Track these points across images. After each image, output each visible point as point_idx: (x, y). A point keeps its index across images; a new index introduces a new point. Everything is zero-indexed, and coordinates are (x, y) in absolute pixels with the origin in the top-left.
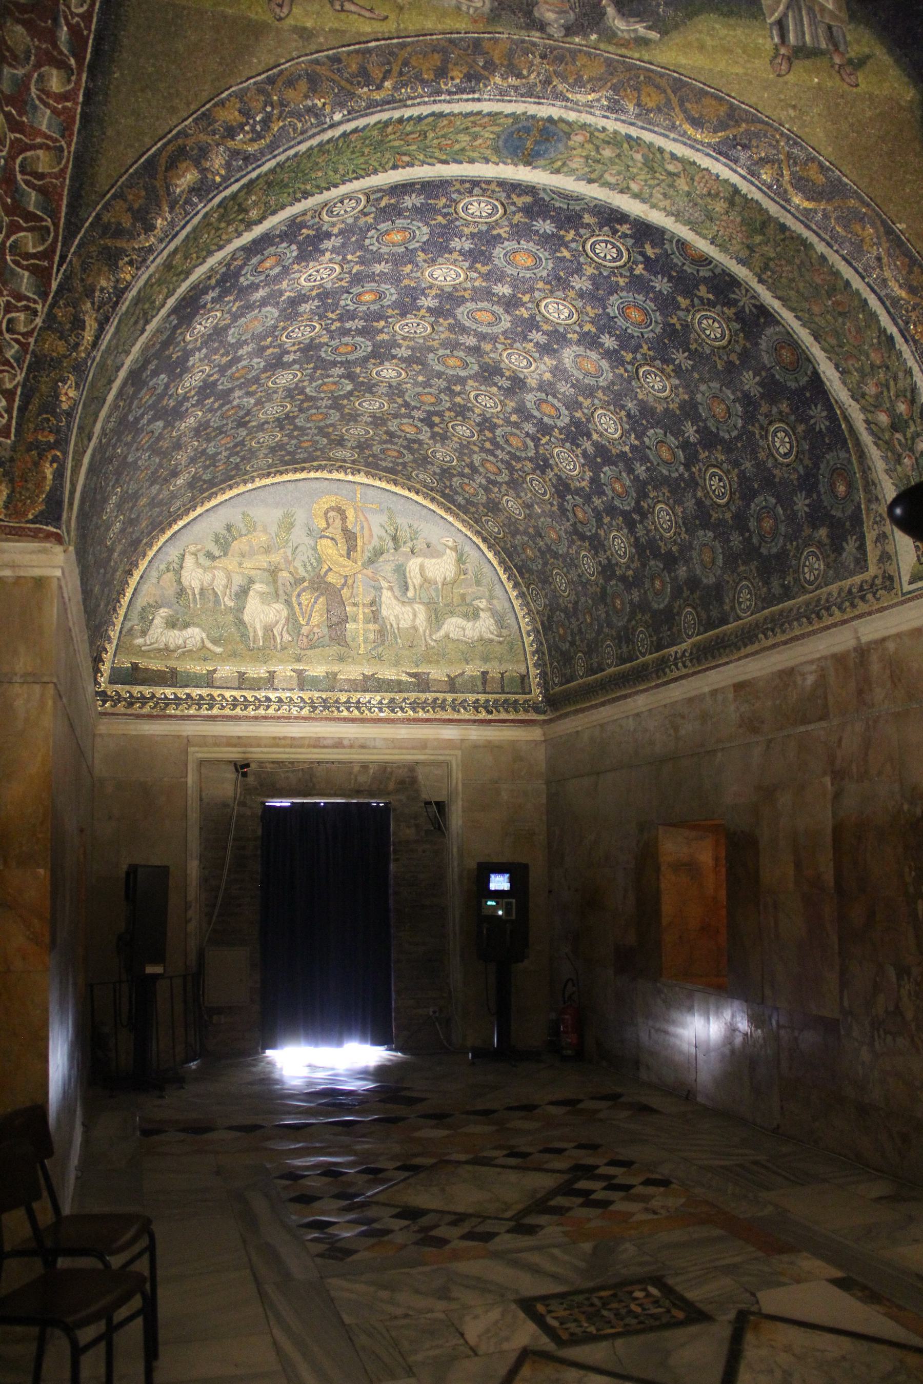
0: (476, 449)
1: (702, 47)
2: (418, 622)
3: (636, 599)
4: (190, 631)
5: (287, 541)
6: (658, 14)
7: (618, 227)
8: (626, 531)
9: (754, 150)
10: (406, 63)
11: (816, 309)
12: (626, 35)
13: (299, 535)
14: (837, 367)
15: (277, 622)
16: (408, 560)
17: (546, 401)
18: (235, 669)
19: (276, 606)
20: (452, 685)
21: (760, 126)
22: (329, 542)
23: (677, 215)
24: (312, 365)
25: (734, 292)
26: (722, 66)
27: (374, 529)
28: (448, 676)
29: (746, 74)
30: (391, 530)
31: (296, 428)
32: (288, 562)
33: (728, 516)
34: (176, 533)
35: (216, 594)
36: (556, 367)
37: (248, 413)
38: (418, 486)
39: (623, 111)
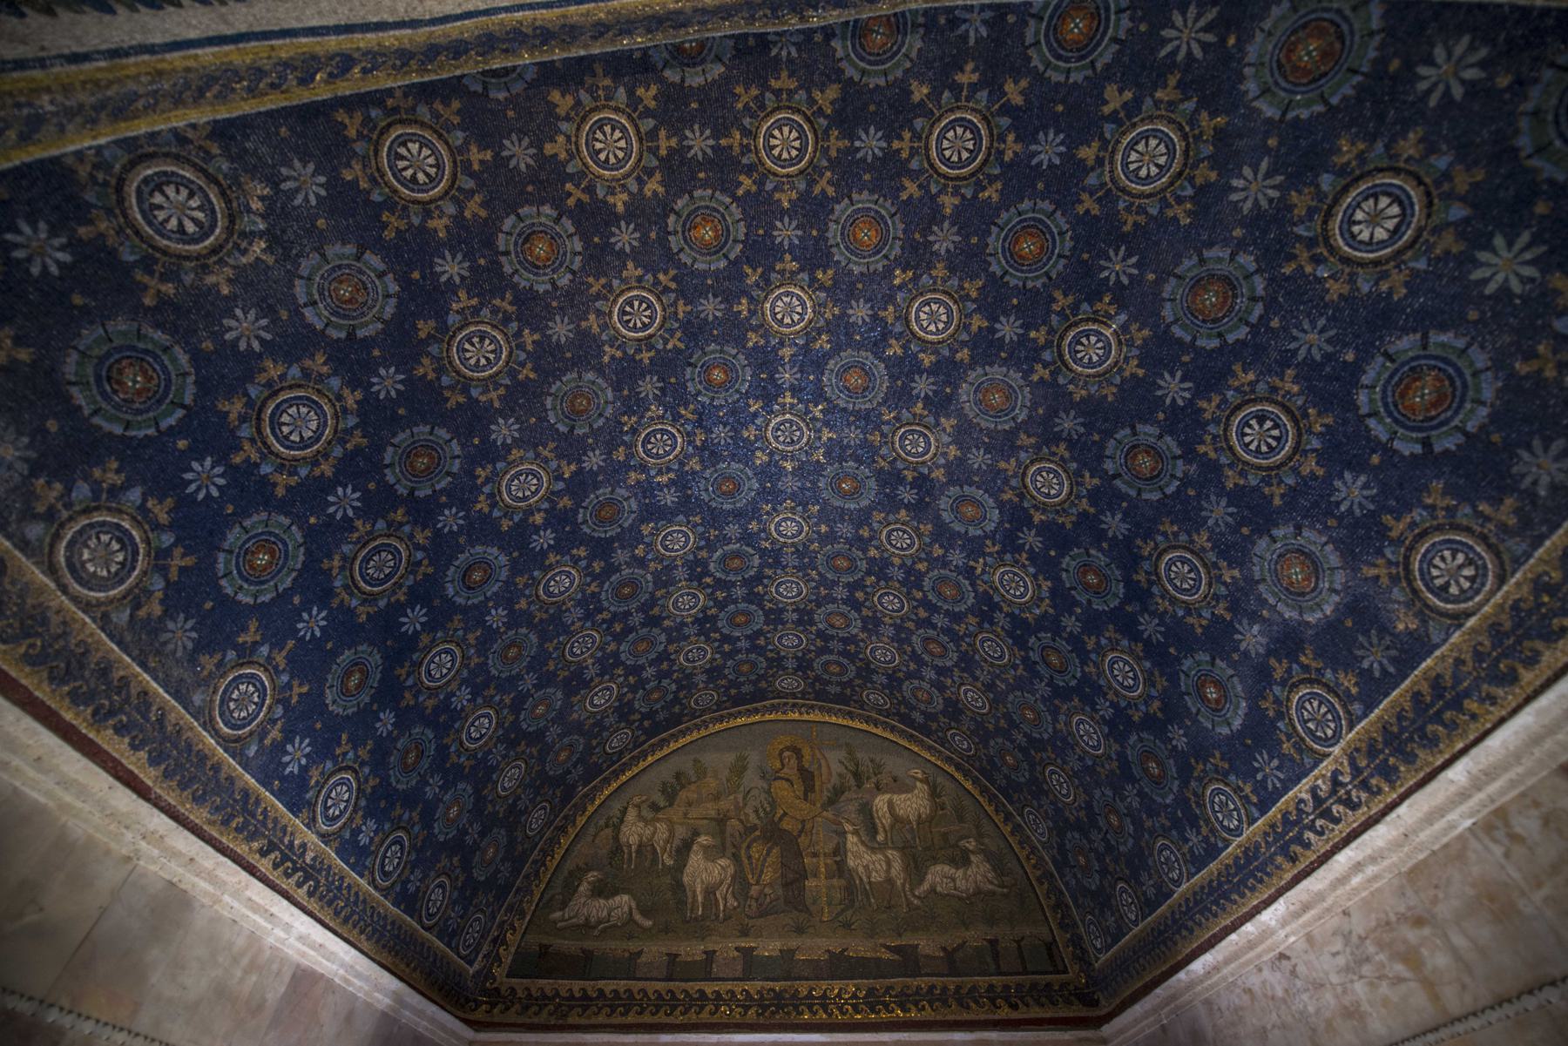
0: (910, 625)
2: (894, 872)
3: (1181, 742)
4: (617, 898)
8: (1125, 643)
13: (751, 779)
16: (874, 797)
17: (963, 499)
18: (664, 950)
19: (723, 862)
20: (952, 962)
22: (786, 785)
24: (698, 519)
27: (833, 764)
28: (944, 949)
31: (726, 639)
32: (737, 808)
33: (1310, 466)
36: (957, 428)
37: (653, 601)
38: (874, 715)
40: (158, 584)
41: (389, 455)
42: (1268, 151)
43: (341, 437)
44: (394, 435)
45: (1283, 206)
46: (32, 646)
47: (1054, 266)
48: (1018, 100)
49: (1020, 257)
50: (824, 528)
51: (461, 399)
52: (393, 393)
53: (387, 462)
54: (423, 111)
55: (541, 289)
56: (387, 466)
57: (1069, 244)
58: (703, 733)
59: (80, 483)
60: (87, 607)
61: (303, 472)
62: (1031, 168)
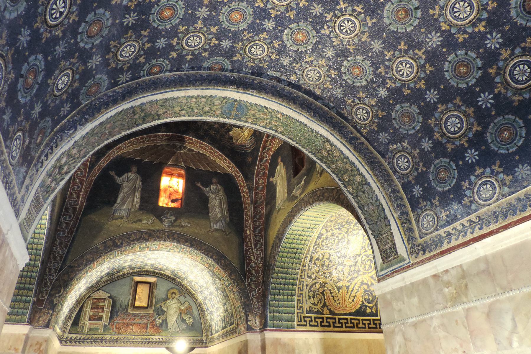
7: (192, 57)
11: (108, 126)
14: (87, 133)
25: (130, 74)
40: (501, 176)
41: (463, 86)
42: (94, 70)
43: (457, 108)
44: (453, 86)
45: (85, 63)
46: (501, 217)
47: (156, 9)
48: (172, 53)
49: (169, 9)
51: (428, 65)
52: (436, 92)
53: (466, 86)
54: (350, 117)
55: (368, 63)
56: (468, 85)
57: (151, 18)
59: (465, 193)
60: (497, 200)
61: (472, 120)
62: (167, 37)
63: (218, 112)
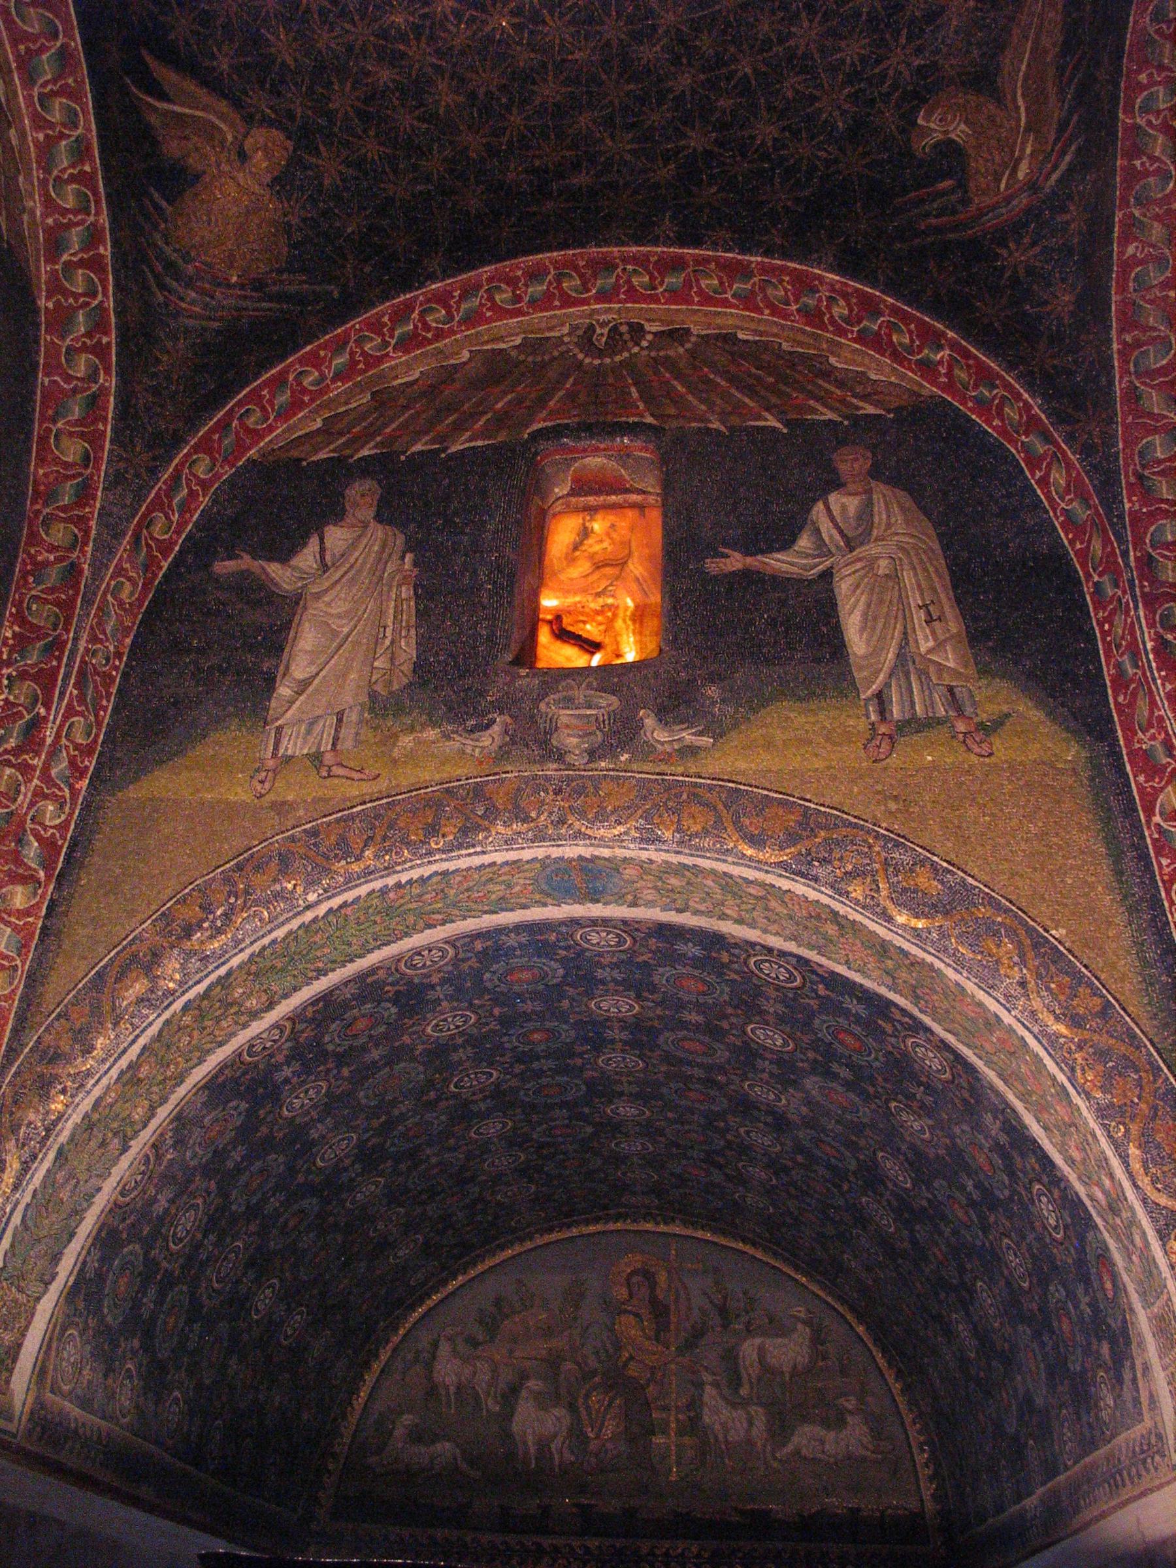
1: (769, 745)
2: (755, 1432)
4: (439, 1446)
5: (575, 1319)
6: (713, 715)
9: (836, 863)
10: (391, 826)
12: (668, 748)
15: (555, 1436)
19: (557, 1412)
21: (844, 831)
23: (794, 938)
26: (796, 763)
29: (829, 768)
30: (718, 1298)
34: (430, 1309)
35: (476, 1397)
39: (659, 839)
50: (670, 1115)
58: (529, 1245)
63: (629, 872)
